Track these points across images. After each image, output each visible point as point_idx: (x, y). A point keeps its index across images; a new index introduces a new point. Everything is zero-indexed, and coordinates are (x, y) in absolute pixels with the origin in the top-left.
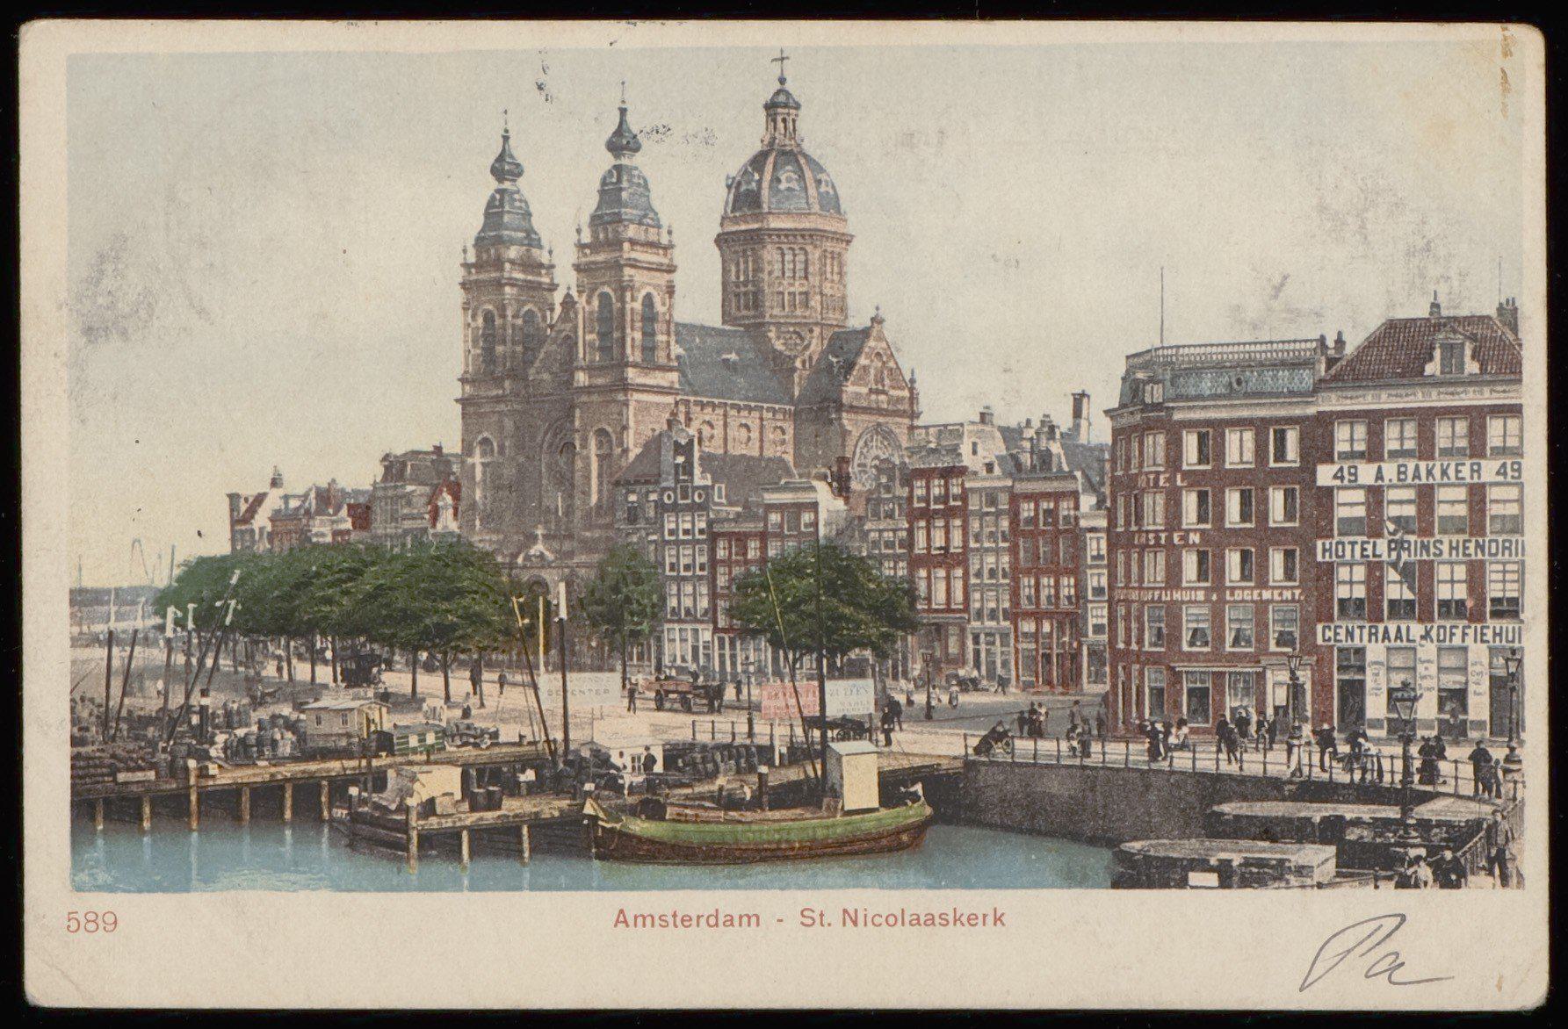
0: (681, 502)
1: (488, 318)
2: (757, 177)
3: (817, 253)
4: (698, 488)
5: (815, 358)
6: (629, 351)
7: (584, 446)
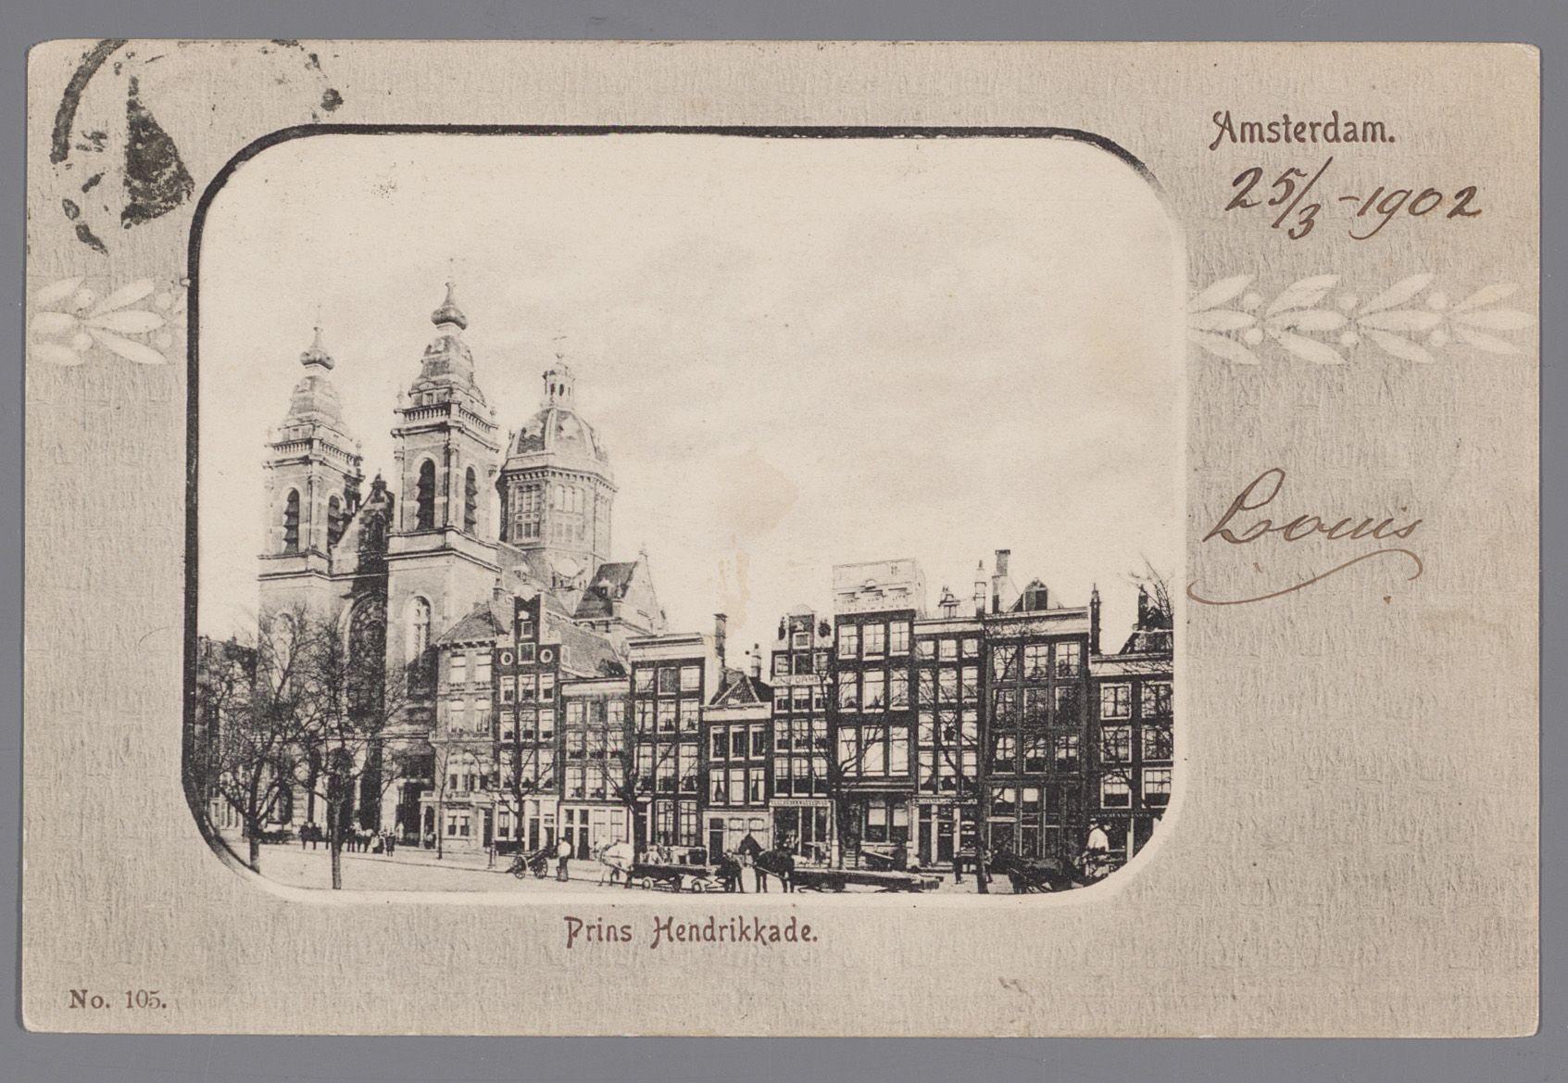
0: (520, 663)
1: (294, 497)
2: (541, 425)
3: (592, 495)
4: (544, 647)
5: (588, 584)
6: (452, 516)
7: (399, 614)
